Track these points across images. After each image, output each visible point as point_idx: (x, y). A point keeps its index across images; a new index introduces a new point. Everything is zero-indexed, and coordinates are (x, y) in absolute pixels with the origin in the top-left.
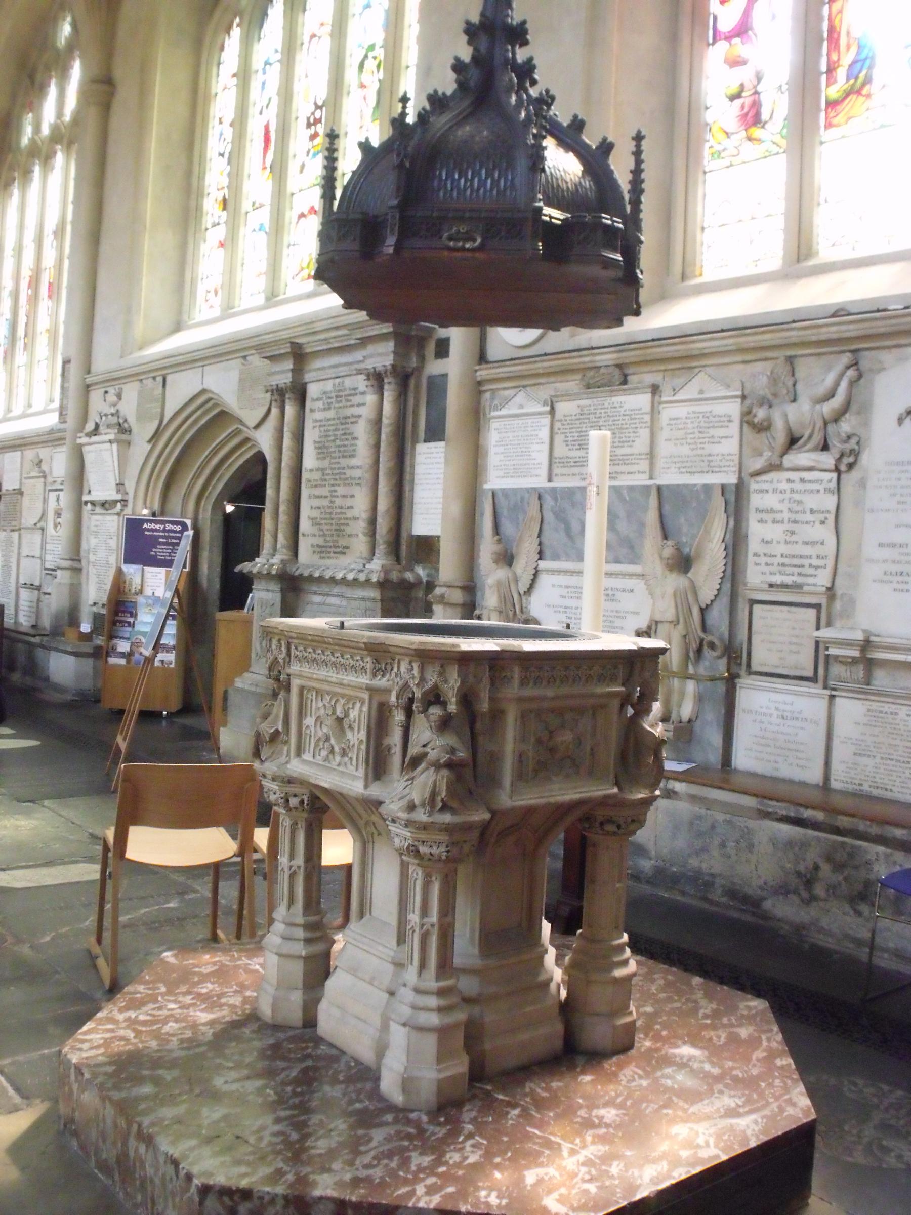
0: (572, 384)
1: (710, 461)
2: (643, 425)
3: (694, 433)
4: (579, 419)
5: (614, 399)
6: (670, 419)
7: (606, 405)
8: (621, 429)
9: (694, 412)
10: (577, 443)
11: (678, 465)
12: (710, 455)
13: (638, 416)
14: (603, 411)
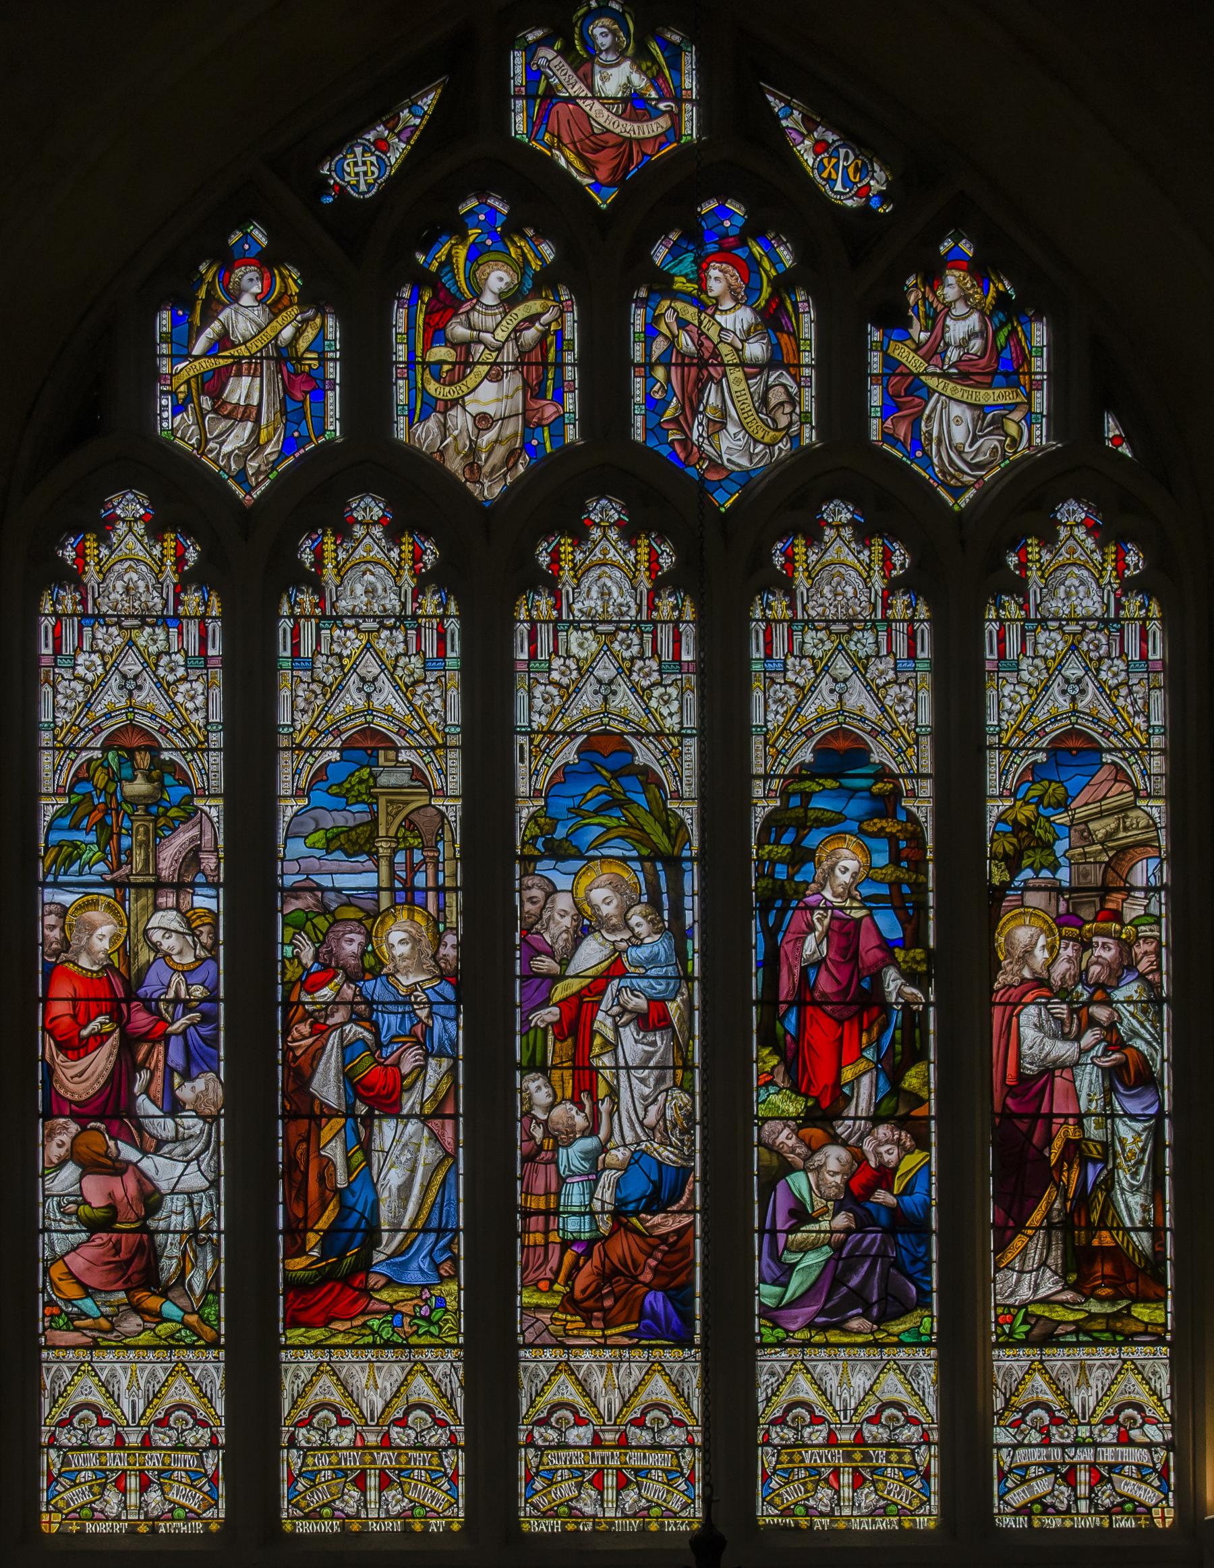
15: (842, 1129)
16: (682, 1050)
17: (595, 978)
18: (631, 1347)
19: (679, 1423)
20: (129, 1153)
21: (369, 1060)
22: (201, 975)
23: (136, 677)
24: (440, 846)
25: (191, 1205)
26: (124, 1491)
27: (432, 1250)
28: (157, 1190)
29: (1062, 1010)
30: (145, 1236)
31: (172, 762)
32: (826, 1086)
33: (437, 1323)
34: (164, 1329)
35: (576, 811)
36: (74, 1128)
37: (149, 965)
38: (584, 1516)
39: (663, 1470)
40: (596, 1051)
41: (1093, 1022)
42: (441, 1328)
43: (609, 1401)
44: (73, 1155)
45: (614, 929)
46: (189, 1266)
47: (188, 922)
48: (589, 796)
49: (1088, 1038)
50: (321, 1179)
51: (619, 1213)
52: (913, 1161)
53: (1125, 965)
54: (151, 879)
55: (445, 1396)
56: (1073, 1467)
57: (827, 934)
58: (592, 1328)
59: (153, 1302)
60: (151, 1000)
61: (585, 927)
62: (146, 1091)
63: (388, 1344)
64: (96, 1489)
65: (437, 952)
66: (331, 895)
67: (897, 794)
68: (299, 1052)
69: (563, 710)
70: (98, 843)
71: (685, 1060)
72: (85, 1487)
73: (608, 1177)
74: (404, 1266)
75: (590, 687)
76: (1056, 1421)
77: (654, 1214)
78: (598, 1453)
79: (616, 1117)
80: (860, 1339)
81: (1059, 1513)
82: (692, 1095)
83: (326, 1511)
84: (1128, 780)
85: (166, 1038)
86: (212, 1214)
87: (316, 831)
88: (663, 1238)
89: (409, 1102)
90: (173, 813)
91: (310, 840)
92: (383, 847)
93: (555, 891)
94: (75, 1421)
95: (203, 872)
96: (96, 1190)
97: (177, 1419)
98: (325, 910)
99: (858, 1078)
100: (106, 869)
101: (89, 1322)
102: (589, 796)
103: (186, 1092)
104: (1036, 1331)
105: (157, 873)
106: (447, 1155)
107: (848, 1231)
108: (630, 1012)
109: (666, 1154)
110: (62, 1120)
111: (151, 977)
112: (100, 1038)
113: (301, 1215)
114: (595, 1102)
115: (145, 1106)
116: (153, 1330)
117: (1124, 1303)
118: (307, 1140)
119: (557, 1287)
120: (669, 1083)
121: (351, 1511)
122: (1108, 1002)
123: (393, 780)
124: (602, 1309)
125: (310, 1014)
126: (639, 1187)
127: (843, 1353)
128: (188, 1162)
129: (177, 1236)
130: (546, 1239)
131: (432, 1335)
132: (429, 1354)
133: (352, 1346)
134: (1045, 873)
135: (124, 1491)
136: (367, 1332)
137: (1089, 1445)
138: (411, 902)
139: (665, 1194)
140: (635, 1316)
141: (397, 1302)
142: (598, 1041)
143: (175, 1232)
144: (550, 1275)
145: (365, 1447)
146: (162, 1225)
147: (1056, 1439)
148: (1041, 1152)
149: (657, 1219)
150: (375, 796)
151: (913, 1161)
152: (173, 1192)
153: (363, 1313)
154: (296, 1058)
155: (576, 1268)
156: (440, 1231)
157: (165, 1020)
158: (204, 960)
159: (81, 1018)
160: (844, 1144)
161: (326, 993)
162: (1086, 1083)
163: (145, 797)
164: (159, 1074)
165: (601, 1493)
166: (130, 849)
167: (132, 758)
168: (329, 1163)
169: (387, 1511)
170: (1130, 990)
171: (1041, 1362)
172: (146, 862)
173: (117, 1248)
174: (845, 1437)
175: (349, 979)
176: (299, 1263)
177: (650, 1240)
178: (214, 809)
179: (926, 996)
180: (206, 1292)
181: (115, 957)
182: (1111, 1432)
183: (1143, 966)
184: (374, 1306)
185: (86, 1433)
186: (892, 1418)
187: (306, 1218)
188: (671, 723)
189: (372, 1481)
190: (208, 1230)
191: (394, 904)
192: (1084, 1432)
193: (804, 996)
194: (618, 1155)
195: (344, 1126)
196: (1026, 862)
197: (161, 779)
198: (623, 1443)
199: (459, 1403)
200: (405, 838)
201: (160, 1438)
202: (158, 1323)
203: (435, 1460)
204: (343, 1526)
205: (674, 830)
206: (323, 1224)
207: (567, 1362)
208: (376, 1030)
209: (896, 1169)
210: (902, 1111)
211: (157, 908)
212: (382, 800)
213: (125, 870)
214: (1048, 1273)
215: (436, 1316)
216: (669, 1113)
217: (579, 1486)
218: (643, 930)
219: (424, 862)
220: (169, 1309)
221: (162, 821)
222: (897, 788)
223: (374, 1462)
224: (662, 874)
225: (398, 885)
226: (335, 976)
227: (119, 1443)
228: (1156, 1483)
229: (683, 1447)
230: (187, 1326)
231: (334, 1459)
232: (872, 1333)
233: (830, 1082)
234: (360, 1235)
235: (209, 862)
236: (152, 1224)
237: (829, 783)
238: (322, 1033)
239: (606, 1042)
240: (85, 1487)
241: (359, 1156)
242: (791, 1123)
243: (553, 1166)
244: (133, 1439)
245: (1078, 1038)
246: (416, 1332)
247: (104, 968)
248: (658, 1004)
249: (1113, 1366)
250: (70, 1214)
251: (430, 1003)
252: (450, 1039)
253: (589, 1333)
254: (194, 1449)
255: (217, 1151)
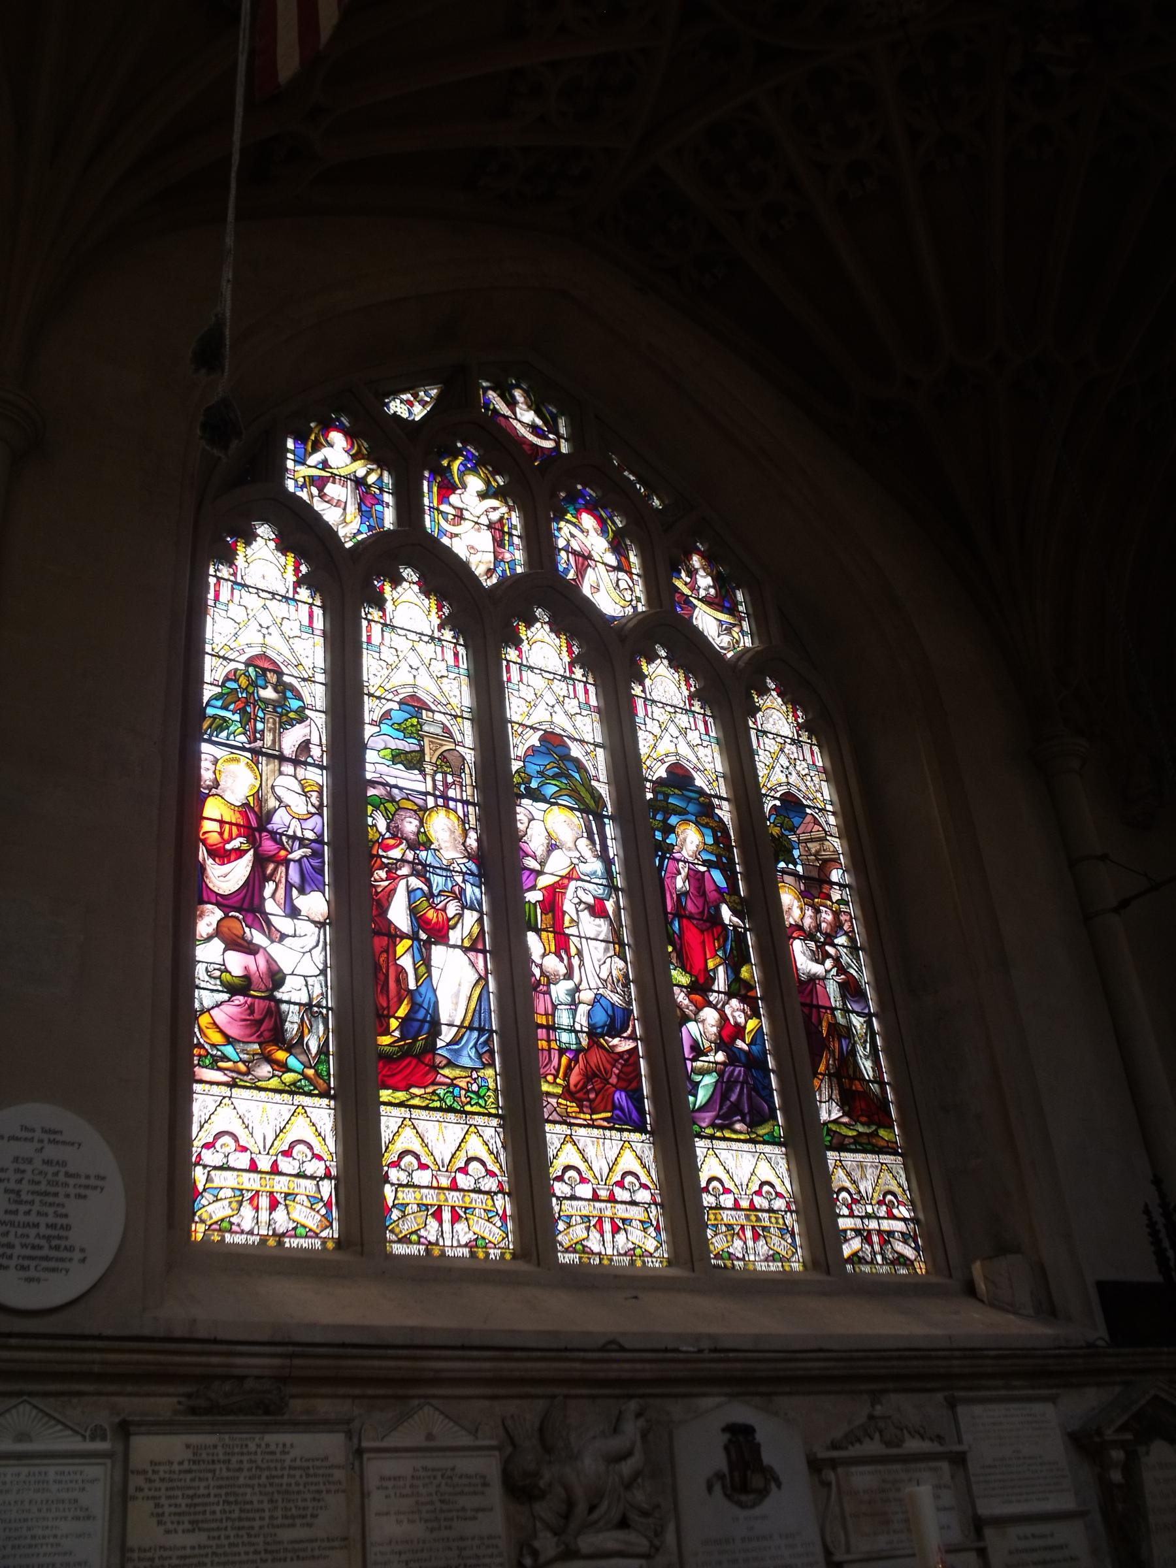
0: (164, 1403)
1: (460, 1549)
2: (333, 1488)
3: (432, 1503)
4: (190, 1471)
5: (268, 1438)
6: (382, 1478)
7: (252, 1447)
8: (287, 1492)
9: (425, 1469)
10: (186, 1519)
11: (404, 1557)
12: (462, 1539)
13: (321, 1472)
14: (245, 1458)
15: (713, 997)
16: (616, 931)
17: (562, 877)
18: (610, 1129)
19: (645, 1187)
20: (258, 938)
21: (425, 904)
22: (309, 824)
23: (267, 628)
24: (463, 775)
25: (307, 985)
26: (257, 1209)
27: (475, 1045)
28: (280, 970)
29: (812, 944)
30: (272, 1003)
31: (291, 685)
32: (700, 970)
33: (483, 1097)
34: (289, 1077)
35: (541, 773)
36: (219, 914)
37: (276, 810)
38: (592, 1253)
39: (640, 1221)
40: (567, 924)
41: (828, 955)
42: (486, 1101)
43: (600, 1166)
44: (218, 933)
45: (570, 849)
46: (306, 1031)
47: (303, 788)
48: (548, 767)
49: (829, 963)
50: (398, 981)
51: (593, 1033)
52: (752, 1024)
53: (837, 926)
54: (277, 753)
55: (492, 1153)
56: (869, 1231)
57: (688, 877)
58: (584, 1113)
59: (281, 1055)
60: (276, 833)
61: (552, 847)
62: (273, 896)
63: (450, 1109)
64: (235, 1205)
65: (465, 841)
66: (395, 791)
67: (712, 807)
68: (379, 890)
69: (529, 715)
70: (240, 722)
71: (619, 938)
72: (226, 1202)
73: (583, 1009)
74: (457, 1053)
75: (542, 706)
76: (855, 1201)
77: (613, 1038)
78: (598, 1205)
79: (583, 969)
80: (742, 1137)
81: (867, 1263)
82: (626, 962)
83: (414, 1237)
84: (820, 825)
85: (286, 862)
86: (322, 994)
87: (385, 749)
88: (621, 1054)
89: (454, 936)
90: (292, 715)
91: (382, 753)
92: (429, 769)
93: (534, 819)
94: (218, 1145)
95: (312, 757)
96: (237, 963)
97: (299, 1152)
98: (392, 800)
99: (716, 967)
100: (246, 740)
101: (229, 1064)
102: (548, 767)
103: (301, 902)
104: (834, 1141)
105: (280, 750)
106: (481, 978)
107: (723, 1063)
108: (585, 903)
109: (616, 999)
110: (209, 906)
111: (276, 818)
112: (239, 853)
113: (385, 1005)
114: (569, 957)
115: (270, 906)
116: (280, 1077)
117: (874, 1128)
118: (387, 951)
119: (558, 1081)
120: (612, 953)
121: (433, 1239)
122: (834, 945)
123: (432, 730)
124: (589, 1100)
125: (386, 865)
126: (601, 1018)
127: (735, 1145)
128: (304, 953)
129: (297, 1007)
130: (549, 1045)
131: (481, 1106)
132: (479, 1120)
133: (426, 1108)
134: (791, 866)
135: (257, 1209)
136: (436, 1098)
137: (873, 1218)
138: (446, 806)
139: (618, 1025)
140: (609, 1107)
141: (456, 1078)
142: (567, 918)
143: (295, 1004)
144: (553, 1072)
145: (439, 1188)
146: (285, 997)
147: (856, 1213)
148: (817, 1028)
149: (616, 1041)
150: (422, 737)
151: (752, 1024)
152: (292, 974)
153: (434, 1083)
154: (377, 893)
155: (569, 1069)
156: (481, 1030)
157: (286, 849)
158: (313, 814)
159: (226, 836)
160: (715, 1007)
161: (396, 853)
162: (832, 990)
163: (273, 701)
164: (282, 886)
165: (602, 1236)
166: (263, 731)
167: (265, 675)
168: (401, 970)
169: (458, 1241)
170: (841, 940)
171: (840, 1161)
172: (274, 741)
173: (251, 1010)
174: (745, 1204)
175: (411, 847)
176: (385, 1040)
177: (612, 1055)
178: (320, 719)
179: (744, 923)
180: (320, 1052)
181: (251, 799)
182: (883, 1211)
183: (846, 927)
184: (440, 1079)
185: (227, 1156)
186: (768, 1193)
187: (388, 1007)
188: (588, 738)
189: (447, 1215)
190: (319, 1005)
191: (437, 806)
192: (869, 1209)
193: (680, 912)
194: (587, 996)
195: (412, 946)
196: (781, 858)
197: (284, 694)
198: (612, 1199)
199: (502, 1157)
200: (441, 766)
201: (285, 1165)
202: (284, 1073)
203: (490, 1202)
204: (427, 1250)
205: (597, 798)
206: (402, 1012)
207: (571, 1135)
208: (428, 882)
209: (745, 1027)
210: (743, 992)
211: (281, 773)
212: (426, 740)
213: (259, 744)
214: (834, 1104)
215: (482, 1092)
216: (614, 973)
217: (588, 1229)
218: (587, 853)
219: (454, 783)
220: (293, 1062)
221: (284, 719)
222: (711, 802)
223: (446, 1200)
224: (593, 822)
225: (438, 793)
226: (401, 843)
227: (253, 1168)
228: (913, 1245)
229: (650, 1204)
230: (306, 1077)
231: (418, 1196)
232: (748, 1133)
233: (702, 967)
234: (426, 1026)
235: (316, 752)
236: (278, 995)
237: (676, 791)
238: (394, 879)
239: (572, 920)
240: (226, 1202)
241: (422, 969)
242: (685, 990)
243: (547, 996)
244: (264, 1164)
245: (823, 963)
246: (469, 1103)
247: (243, 805)
248: (600, 901)
249: (877, 1167)
250: (215, 978)
251: (464, 874)
252: (476, 899)
253: (582, 1116)
254: (312, 1177)
255: (325, 949)
